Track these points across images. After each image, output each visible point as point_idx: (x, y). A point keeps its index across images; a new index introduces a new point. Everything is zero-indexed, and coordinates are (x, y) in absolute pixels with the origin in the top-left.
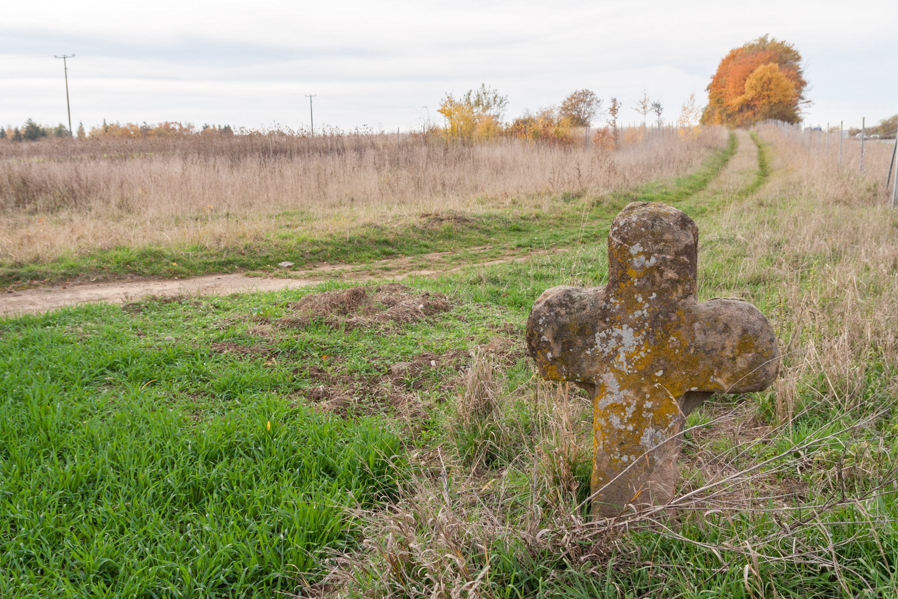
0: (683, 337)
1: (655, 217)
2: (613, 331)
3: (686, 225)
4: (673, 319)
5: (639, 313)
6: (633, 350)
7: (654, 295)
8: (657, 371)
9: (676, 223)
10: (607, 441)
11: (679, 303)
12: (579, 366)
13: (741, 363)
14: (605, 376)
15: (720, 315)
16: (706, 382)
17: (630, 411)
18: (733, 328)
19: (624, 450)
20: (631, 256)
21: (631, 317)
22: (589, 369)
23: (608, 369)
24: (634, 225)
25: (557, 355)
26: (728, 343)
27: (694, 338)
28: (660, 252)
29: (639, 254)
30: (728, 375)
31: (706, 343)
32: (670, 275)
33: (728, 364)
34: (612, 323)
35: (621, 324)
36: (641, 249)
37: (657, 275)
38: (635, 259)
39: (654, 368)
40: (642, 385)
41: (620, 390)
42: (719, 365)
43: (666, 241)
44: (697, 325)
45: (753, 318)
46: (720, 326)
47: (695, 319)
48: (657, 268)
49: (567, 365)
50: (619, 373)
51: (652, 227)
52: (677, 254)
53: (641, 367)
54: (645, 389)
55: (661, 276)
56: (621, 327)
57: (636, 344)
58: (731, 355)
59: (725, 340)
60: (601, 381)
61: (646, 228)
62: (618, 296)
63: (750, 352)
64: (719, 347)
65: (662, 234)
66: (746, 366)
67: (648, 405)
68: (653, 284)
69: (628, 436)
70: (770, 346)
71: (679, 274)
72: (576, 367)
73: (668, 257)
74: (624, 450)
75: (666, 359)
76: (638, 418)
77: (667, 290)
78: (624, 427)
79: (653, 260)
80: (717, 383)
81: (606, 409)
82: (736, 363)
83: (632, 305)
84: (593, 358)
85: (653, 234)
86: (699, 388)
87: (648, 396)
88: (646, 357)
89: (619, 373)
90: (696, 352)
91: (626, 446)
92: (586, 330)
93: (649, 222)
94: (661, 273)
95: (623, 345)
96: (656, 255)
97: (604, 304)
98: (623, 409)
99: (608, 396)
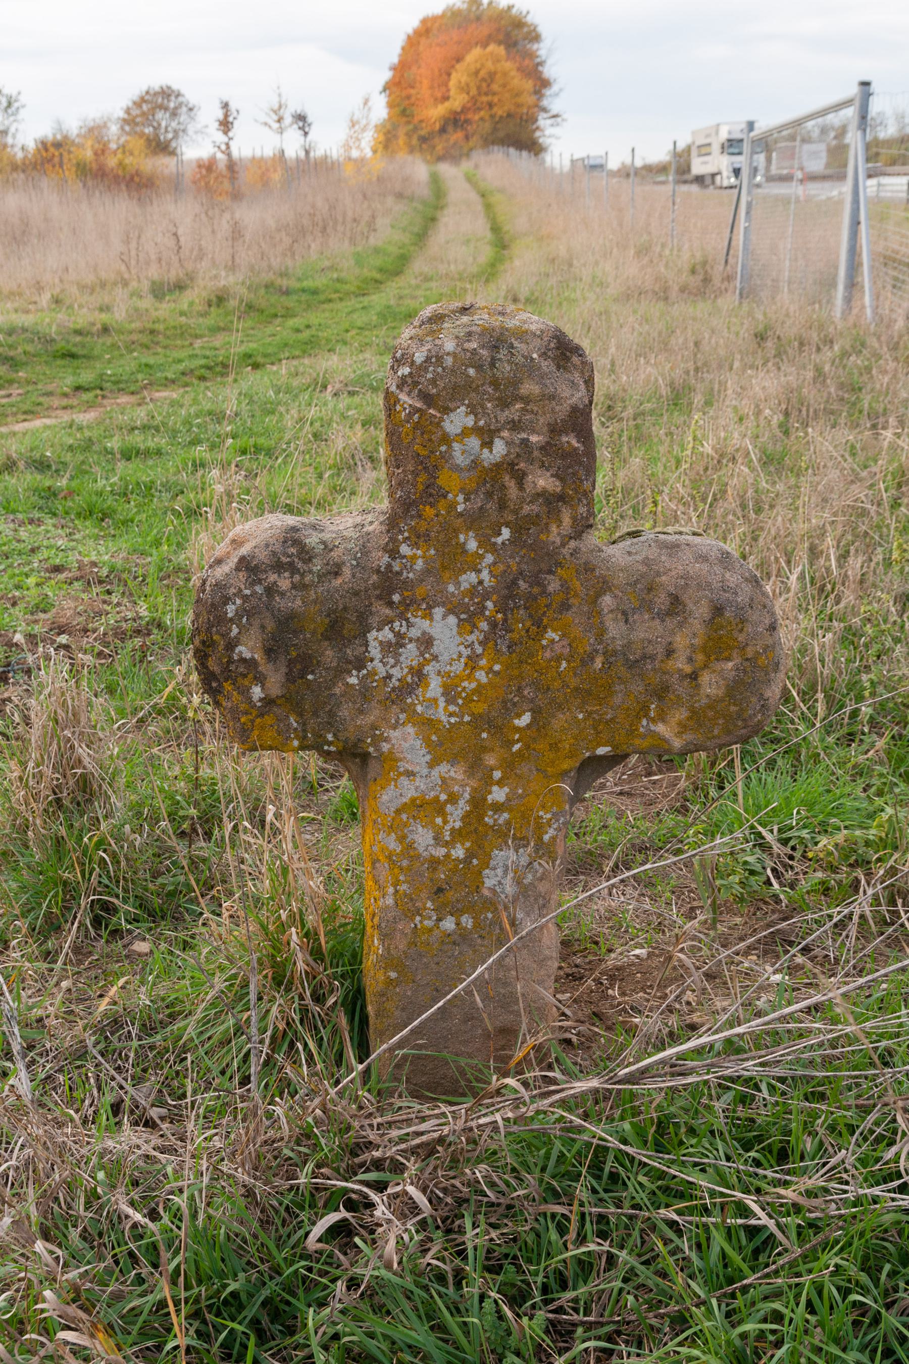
0: (577, 631)
1: (497, 340)
2: (410, 625)
3: (568, 359)
4: (551, 589)
5: (472, 577)
6: (458, 667)
7: (506, 533)
8: (519, 716)
9: (544, 355)
10: (403, 887)
11: (565, 551)
12: (332, 714)
13: (711, 685)
14: (394, 734)
15: (658, 574)
16: (632, 732)
17: (456, 814)
18: (691, 606)
19: (445, 905)
20: (446, 439)
21: (451, 588)
22: (354, 721)
23: (403, 717)
24: (449, 361)
25: (275, 691)
26: (681, 641)
27: (602, 632)
28: (515, 426)
29: (465, 432)
30: (681, 714)
31: (630, 643)
32: (541, 483)
33: (681, 689)
34: (408, 604)
35: (430, 608)
36: (470, 421)
37: (511, 484)
38: (456, 446)
39: (510, 709)
40: (484, 749)
41: (431, 765)
42: (661, 692)
43: (526, 400)
44: (607, 601)
45: (733, 579)
46: (661, 601)
47: (604, 586)
48: (509, 466)
49: (300, 715)
50: (427, 724)
51: (493, 365)
52: (554, 430)
53: (480, 708)
54: (490, 760)
55: (521, 486)
56: (429, 616)
57: (466, 652)
58: (688, 669)
59: (673, 633)
60: (385, 747)
61: (479, 368)
62: (418, 538)
63: (728, 659)
64: (660, 650)
65: (515, 383)
66: (720, 693)
67: (498, 794)
68: (502, 505)
69: (454, 871)
70: (770, 642)
71: (561, 479)
72: (323, 717)
73: (534, 439)
74: (445, 905)
75: (536, 685)
76: (478, 831)
77: (534, 520)
78: (442, 851)
79: (499, 448)
80: (653, 734)
81: (398, 812)
82: (698, 686)
83: (453, 560)
84: (365, 693)
85: (495, 383)
86: (615, 747)
87: (497, 775)
88: (490, 682)
89: (427, 724)
90: (608, 665)
91: (451, 895)
92: (344, 627)
93: (484, 352)
94: (520, 478)
95: (435, 658)
96: (505, 434)
97: (386, 559)
98: (440, 810)
99: (404, 781)
